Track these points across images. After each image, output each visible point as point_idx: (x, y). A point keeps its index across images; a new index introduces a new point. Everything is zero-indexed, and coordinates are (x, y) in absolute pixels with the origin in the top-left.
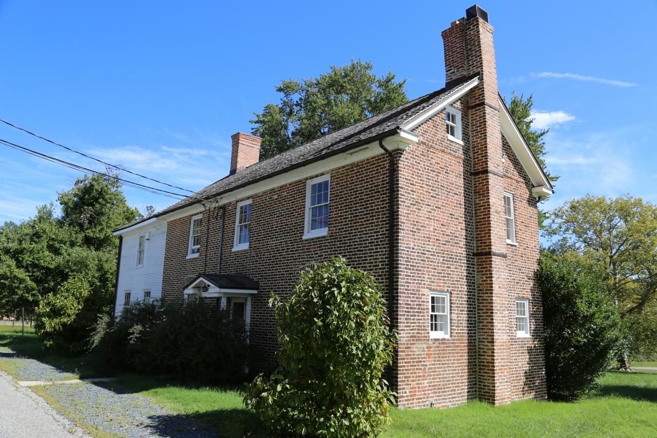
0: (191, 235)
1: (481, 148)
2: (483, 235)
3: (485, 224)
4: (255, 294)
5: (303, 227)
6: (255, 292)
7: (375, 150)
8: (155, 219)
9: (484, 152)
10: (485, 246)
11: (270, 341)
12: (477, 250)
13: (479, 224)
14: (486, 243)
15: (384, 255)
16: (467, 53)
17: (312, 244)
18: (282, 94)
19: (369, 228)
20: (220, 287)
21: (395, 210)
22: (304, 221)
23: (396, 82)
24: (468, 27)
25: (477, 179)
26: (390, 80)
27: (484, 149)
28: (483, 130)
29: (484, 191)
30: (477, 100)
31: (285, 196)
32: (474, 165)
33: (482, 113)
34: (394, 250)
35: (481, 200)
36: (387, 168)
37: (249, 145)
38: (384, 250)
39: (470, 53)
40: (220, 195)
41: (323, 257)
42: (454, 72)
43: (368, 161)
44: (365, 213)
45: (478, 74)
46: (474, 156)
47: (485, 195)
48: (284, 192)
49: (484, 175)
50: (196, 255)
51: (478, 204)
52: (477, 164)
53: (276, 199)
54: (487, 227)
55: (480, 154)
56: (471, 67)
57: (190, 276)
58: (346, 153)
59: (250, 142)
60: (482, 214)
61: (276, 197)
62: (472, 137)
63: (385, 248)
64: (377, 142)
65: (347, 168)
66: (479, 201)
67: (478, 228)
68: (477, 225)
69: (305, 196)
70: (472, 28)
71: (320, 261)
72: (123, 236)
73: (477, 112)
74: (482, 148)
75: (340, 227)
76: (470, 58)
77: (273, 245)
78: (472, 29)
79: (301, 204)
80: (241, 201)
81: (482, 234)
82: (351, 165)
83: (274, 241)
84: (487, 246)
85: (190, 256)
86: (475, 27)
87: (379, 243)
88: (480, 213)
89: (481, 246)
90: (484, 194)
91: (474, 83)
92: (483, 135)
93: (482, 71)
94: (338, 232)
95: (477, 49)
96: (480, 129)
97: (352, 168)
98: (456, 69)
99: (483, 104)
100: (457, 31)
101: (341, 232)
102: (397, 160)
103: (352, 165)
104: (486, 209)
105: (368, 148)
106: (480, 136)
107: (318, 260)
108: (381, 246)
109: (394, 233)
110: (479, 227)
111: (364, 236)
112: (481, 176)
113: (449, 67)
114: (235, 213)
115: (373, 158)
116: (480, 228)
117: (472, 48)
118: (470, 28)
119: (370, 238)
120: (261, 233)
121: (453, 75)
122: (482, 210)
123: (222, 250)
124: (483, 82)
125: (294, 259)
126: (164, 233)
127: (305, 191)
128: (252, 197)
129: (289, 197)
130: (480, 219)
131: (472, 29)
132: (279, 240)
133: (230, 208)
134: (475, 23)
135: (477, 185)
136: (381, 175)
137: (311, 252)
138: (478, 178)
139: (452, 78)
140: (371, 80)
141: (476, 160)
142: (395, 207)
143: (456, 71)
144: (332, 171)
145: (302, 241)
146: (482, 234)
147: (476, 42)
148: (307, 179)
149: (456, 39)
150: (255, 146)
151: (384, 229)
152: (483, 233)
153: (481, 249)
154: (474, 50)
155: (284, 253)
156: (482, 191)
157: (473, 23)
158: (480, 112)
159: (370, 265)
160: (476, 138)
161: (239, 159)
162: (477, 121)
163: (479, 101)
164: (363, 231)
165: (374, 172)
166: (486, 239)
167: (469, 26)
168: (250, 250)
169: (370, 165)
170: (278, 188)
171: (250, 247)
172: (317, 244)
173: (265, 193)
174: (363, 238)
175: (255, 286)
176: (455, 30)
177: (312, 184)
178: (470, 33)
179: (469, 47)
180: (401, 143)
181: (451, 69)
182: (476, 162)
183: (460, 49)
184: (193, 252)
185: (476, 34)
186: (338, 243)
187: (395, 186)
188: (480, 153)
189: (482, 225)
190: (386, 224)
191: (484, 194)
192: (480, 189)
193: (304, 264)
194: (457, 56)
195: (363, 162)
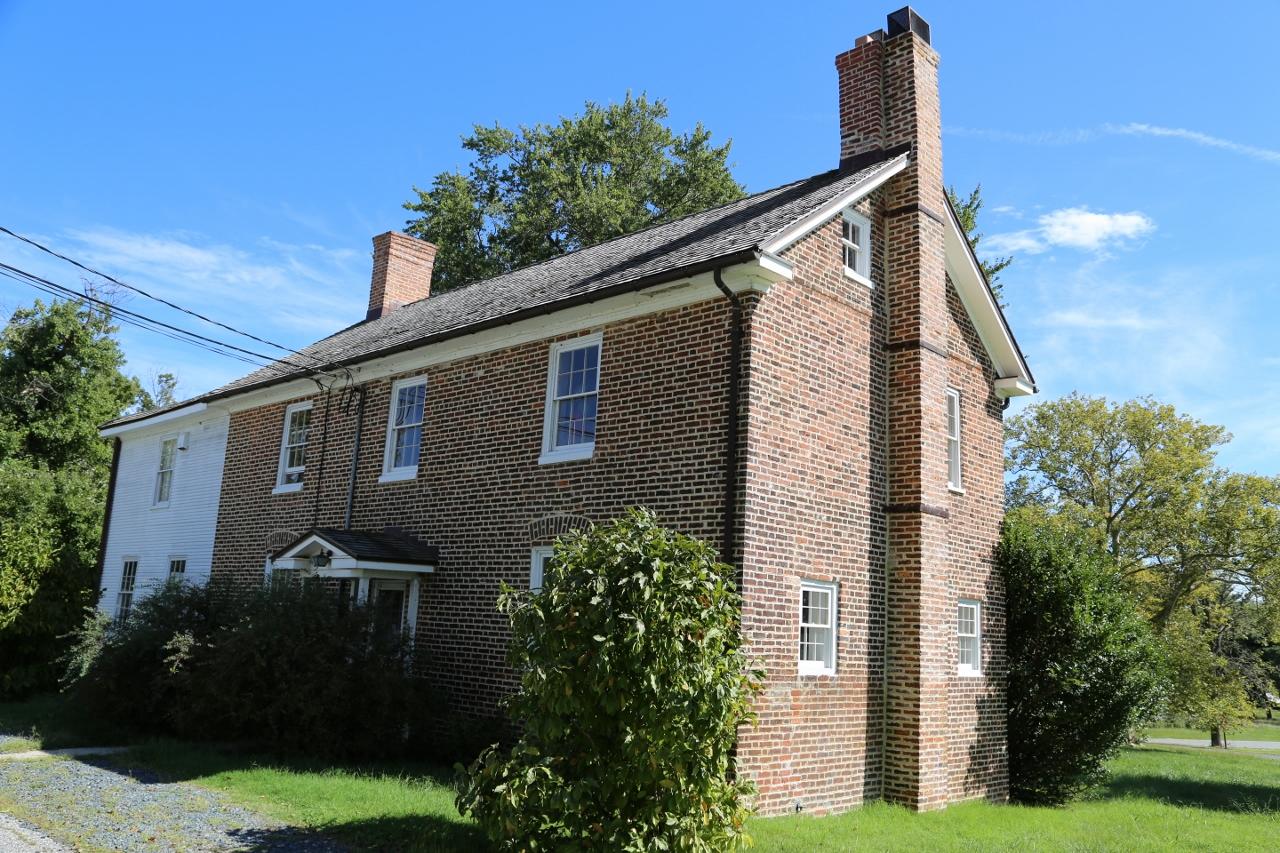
0: (285, 443)
1: (906, 298)
2: (904, 471)
3: (910, 449)
4: (429, 574)
5: (541, 439)
6: (429, 569)
7: (704, 290)
8: (201, 406)
10: (907, 493)
11: (459, 672)
12: (892, 500)
14: (910, 486)
15: (713, 504)
16: (887, 103)
17: (559, 474)
20: (359, 558)
22: (542, 427)
23: (707, 150)
25: (896, 359)
26: (699, 143)
28: (911, 260)
29: (910, 383)
31: (501, 374)
33: (911, 226)
34: (735, 495)
35: (903, 401)
36: (727, 328)
37: (411, 259)
38: (715, 493)
39: (891, 104)
41: (581, 503)
42: (858, 140)
43: (686, 312)
44: (677, 416)
46: (892, 312)
48: (499, 364)
49: (912, 352)
50: (297, 487)
52: (897, 328)
53: (481, 378)
54: (914, 455)
55: (905, 309)
57: (280, 530)
58: (642, 292)
59: (413, 252)
60: (904, 429)
61: (481, 373)
62: (890, 273)
63: (717, 489)
64: (710, 275)
67: (894, 457)
69: (546, 375)
70: (899, 53)
71: (575, 510)
72: (122, 438)
73: (903, 223)
76: (892, 115)
77: (472, 474)
80: (403, 377)
83: (475, 464)
84: (913, 492)
85: (281, 489)
86: (906, 52)
87: (705, 480)
89: (901, 493)
91: (899, 164)
92: (911, 271)
93: (916, 142)
94: (617, 454)
95: (908, 97)
97: (651, 323)
98: (862, 133)
99: (915, 208)
100: (867, 56)
101: (624, 453)
102: (747, 314)
103: (652, 317)
104: (912, 418)
105: (687, 285)
106: (905, 271)
107: (571, 508)
108: (709, 486)
109: (737, 460)
110: (897, 454)
111: (672, 463)
112: (904, 352)
115: (696, 306)
119: (684, 469)
120: (446, 447)
122: (905, 422)
123: (355, 478)
124: (916, 165)
125: (518, 505)
126: (220, 436)
127: (546, 364)
128: (427, 370)
129: (509, 375)
130: (899, 438)
132: (485, 463)
133: (377, 391)
134: (906, 44)
135: (896, 370)
136: (713, 342)
137: (556, 490)
140: (662, 138)
141: (896, 320)
143: (862, 137)
144: (607, 327)
145: (537, 468)
147: (906, 83)
148: (551, 340)
150: (423, 262)
151: (716, 452)
152: (905, 466)
161: (387, 288)
164: (670, 454)
165: (698, 335)
166: (911, 480)
167: (892, 48)
169: (691, 320)
170: (486, 355)
171: (419, 476)
172: (570, 476)
173: (458, 364)
174: (670, 467)
176: (863, 55)
178: (894, 64)
179: (891, 92)
184: (289, 479)
186: (616, 476)
187: (742, 365)
188: (904, 305)
190: (720, 441)
192: (902, 378)
193: (541, 515)
195: (674, 312)
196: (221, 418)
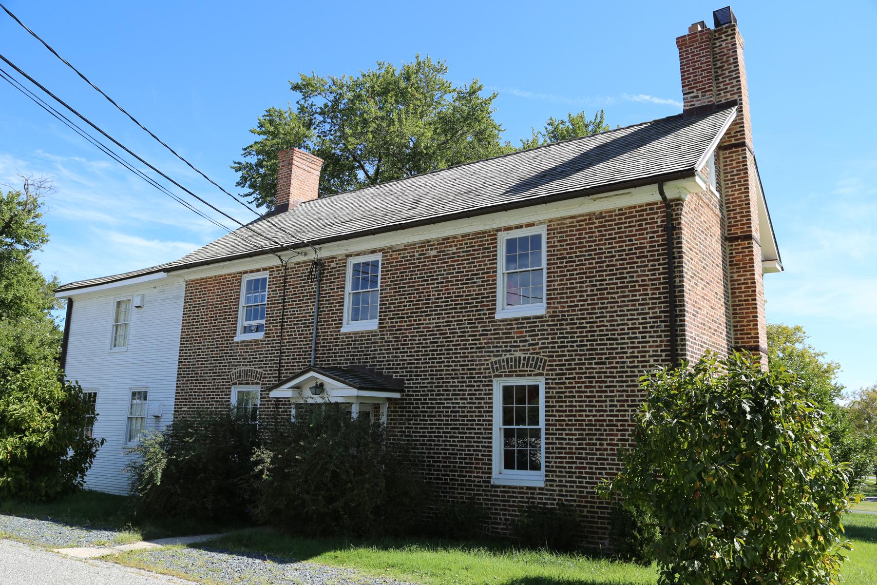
0: (242, 302)
1: (739, 205)
2: (745, 323)
3: (749, 309)
4: (395, 399)
5: (495, 300)
6: (397, 395)
7: (649, 195)
8: (162, 273)
9: (744, 211)
10: (748, 338)
11: (430, 470)
12: (736, 343)
13: (738, 308)
14: (750, 334)
15: (657, 346)
16: (716, 72)
17: (515, 326)
18: (298, 95)
19: (628, 308)
20: (360, 388)
21: (676, 284)
22: (495, 292)
23: (483, 95)
24: (717, 36)
25: (734, 247)
26: (474, 92)
27: (744, 206)
28: (742, 180)
29: (746, 263)
30: (733, 139)
31: (453, 253)
32: (728, 226)
33: (741, 157)
34: (677, 340)
35: (742, 276)
36: (659, 223)
37: (307, 168)
38: (659, 339)
39: (720, 73)
40: (319, 244)
41: (537, 347)
42: (697, 97)
43: (621, 212)
44: (620, 285)
45: (733, 104)
46: (728, 215)
47: (748, 269)
48: (451, 246)
49: (746, 242)
50: (260, 335)
51: (737, 280)
52: (734, 226)
53: (434, 256)
54: (752, 312)
55: (739, 213)
56: (722, 92)
57: (244, 368)
58: (591, 197)
59: (308, 164)
60: (743, 295)
61: (434, 253)
62: (726, 188)
63: (660, 336)
64: (655, 187)
65: (579, 219)
66: (738, 276)
67: (736, 314)
68: (734, 310)
69: (496, 255)
70: (724, 38)
71: (531, 351)
72: (74, 299)
73: (734, 154)
74: (742, 205)
75: (570, 304)
76: (721, 80)
77: (431, 326)
78: (725, 40)
79: (488, 266)
80: (358, 255)
81: (743, 321)
82: (587, 215)
83: (434, 319)
84: (752, 338)
85: (240, 337)
86: (729, 38)
87: (649, 329)
88: (739, 293)
89: (743, 338)
90: (746, 267)
91: (731, 115)
92: (743, 188)
93: (741, 100)
94: (568, 311)
95: (733, 69)
96: (738, 178)
97: (590, 219)
98: (700, 92)
99: (743, 144)
100: (702, 39)
101: (574, 311)
102: (677, 214)
103: (591, 216)
104: (749, 287)
105: (630, 193)
106: (737, 187)
107: (529, 350)
108: (652, 334)
109: (677, 316)
110: (738, 311)
111: (618, 318)
112: (740, 242)
113: (689, 89)
114: (345, 274)
115: (630, 208)
116: (740, 313)
117: (724, 66)
118: (721, 38)
119: (630, 322)
120: (405, 306)
121: (695, 99)
122: (743, 290)
123: (317, 329)
124: (742, 115)
125: (477, 348)
126: (177, 297)
127: (496, 247)
128: (381, 250)
129: (461, 254)
130: (739, 301)
131: (725, 40)
132: (444, 318)
133: (333, 265)
134: (730, 32)
135: (734, 255)
136: (647, 233)
137: (513, 337)
138: (736, 245)
139: (694, 105)
140: (444, 88)
141: (732, 220)
142: (677, 280)
143: (700, 94)
144: (550, 221)
145: (494, 322)
146: (743, 321)
147: (731, 59)
148: (499, 230)
149: (700, 50)
150: (313, 171)
151: (657, 310)
152: (745, 320)
153: (742, 342)
154: (727, 69)
155: (454, 339)
156: (743, 264)
157: (727, 32)
158: (739, 155)
159: (631, 360)
160: (732, 191)
162: (734, 168)
163: (735, 140)
164: (616, 311)
165: (634, 229)
166: (751, 329)
167: (719, 35)
168: (380, 331)
169: (626, 218)
170: (438, 240)
171: (380, 327)
172: (526, 327)
173: (412, 246)
174: (616, 321)
175: (398, 386)
176: (699, 38)
177: (509, 238)
178: (721, 45)
179: (719, 64)
180: (685, 191)
181: (693, 92)
182: (733, 224)
183: (707, 66)
184: (247, 330)
185: (731, 47)
186: (568, 327)
187: (675, 250)
188: (738, 211)
189: (744, 309)
190: (660, 303)
191: (746, 267)
192: (740, 260)
193: (501, 355)
194: (702, 74)
195: (611, 212)
196: (178, 285)
